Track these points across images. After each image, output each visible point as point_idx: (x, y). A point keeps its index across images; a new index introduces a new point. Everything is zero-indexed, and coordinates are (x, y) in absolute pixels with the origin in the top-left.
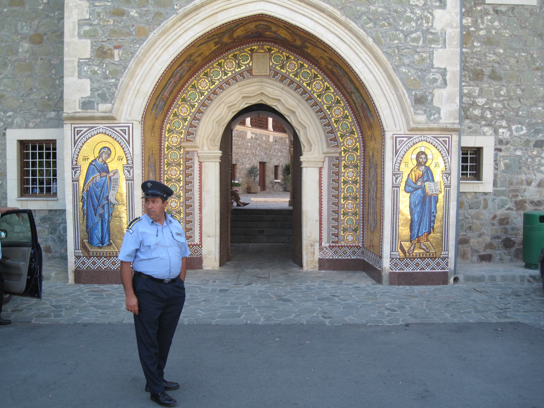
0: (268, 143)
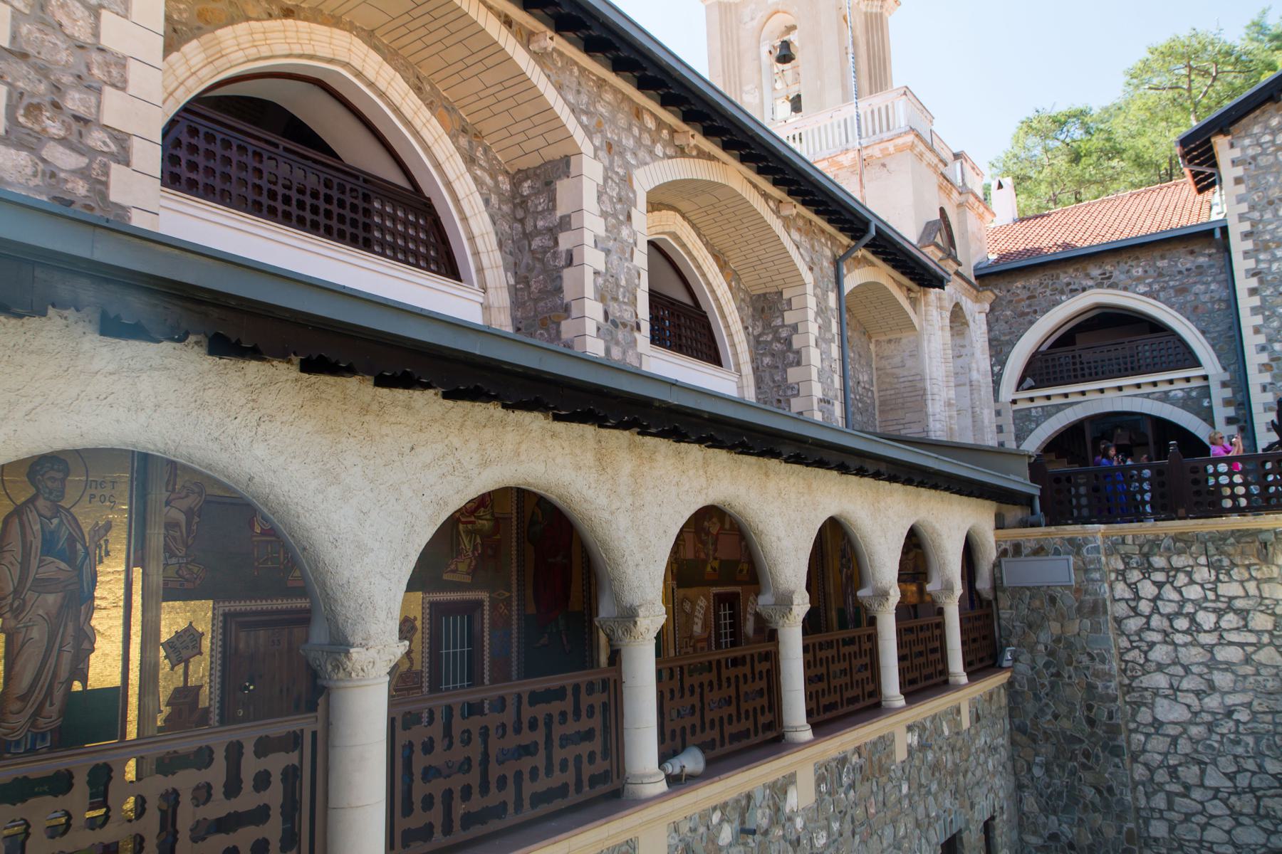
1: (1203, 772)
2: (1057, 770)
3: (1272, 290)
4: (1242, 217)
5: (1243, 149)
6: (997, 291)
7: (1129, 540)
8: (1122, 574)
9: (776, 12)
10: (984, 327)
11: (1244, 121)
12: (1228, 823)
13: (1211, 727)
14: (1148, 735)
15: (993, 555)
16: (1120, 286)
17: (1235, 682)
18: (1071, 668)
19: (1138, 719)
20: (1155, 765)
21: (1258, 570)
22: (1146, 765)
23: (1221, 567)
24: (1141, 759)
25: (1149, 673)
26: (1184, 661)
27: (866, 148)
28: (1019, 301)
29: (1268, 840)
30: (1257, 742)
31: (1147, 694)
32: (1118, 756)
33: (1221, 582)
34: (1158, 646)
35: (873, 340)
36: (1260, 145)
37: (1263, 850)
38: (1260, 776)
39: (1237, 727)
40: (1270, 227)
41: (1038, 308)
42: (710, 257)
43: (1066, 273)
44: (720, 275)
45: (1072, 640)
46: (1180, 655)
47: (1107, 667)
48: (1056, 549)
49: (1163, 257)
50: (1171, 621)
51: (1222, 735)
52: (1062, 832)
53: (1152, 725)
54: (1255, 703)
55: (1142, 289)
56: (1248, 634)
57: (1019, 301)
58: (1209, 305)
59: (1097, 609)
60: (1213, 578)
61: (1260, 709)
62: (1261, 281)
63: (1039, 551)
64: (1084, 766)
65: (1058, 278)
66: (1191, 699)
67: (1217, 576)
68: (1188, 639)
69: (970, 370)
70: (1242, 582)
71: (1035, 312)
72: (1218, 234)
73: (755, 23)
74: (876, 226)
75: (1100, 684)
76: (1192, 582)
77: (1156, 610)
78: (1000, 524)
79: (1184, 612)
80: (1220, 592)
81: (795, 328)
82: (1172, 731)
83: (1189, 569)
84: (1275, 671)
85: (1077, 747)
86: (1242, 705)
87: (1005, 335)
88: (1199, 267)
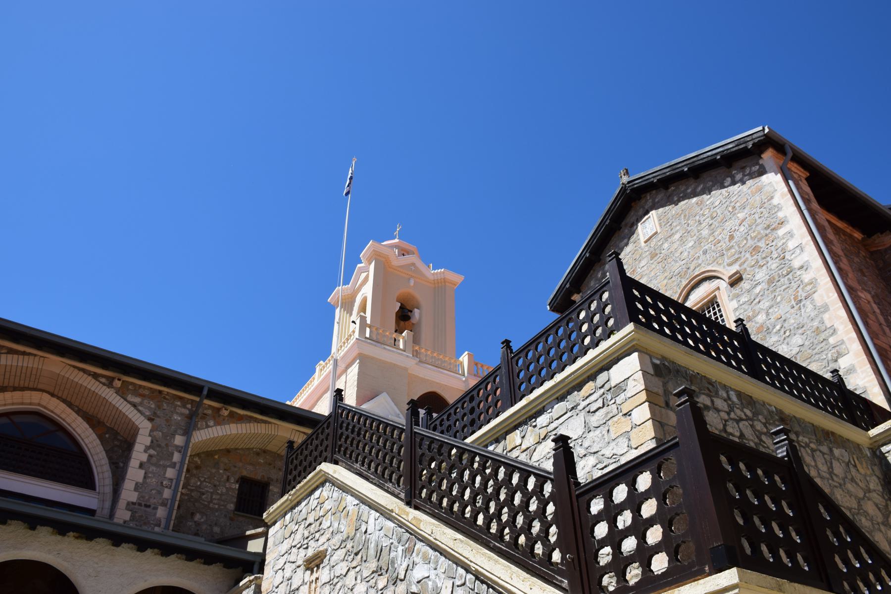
42: (80, 419)
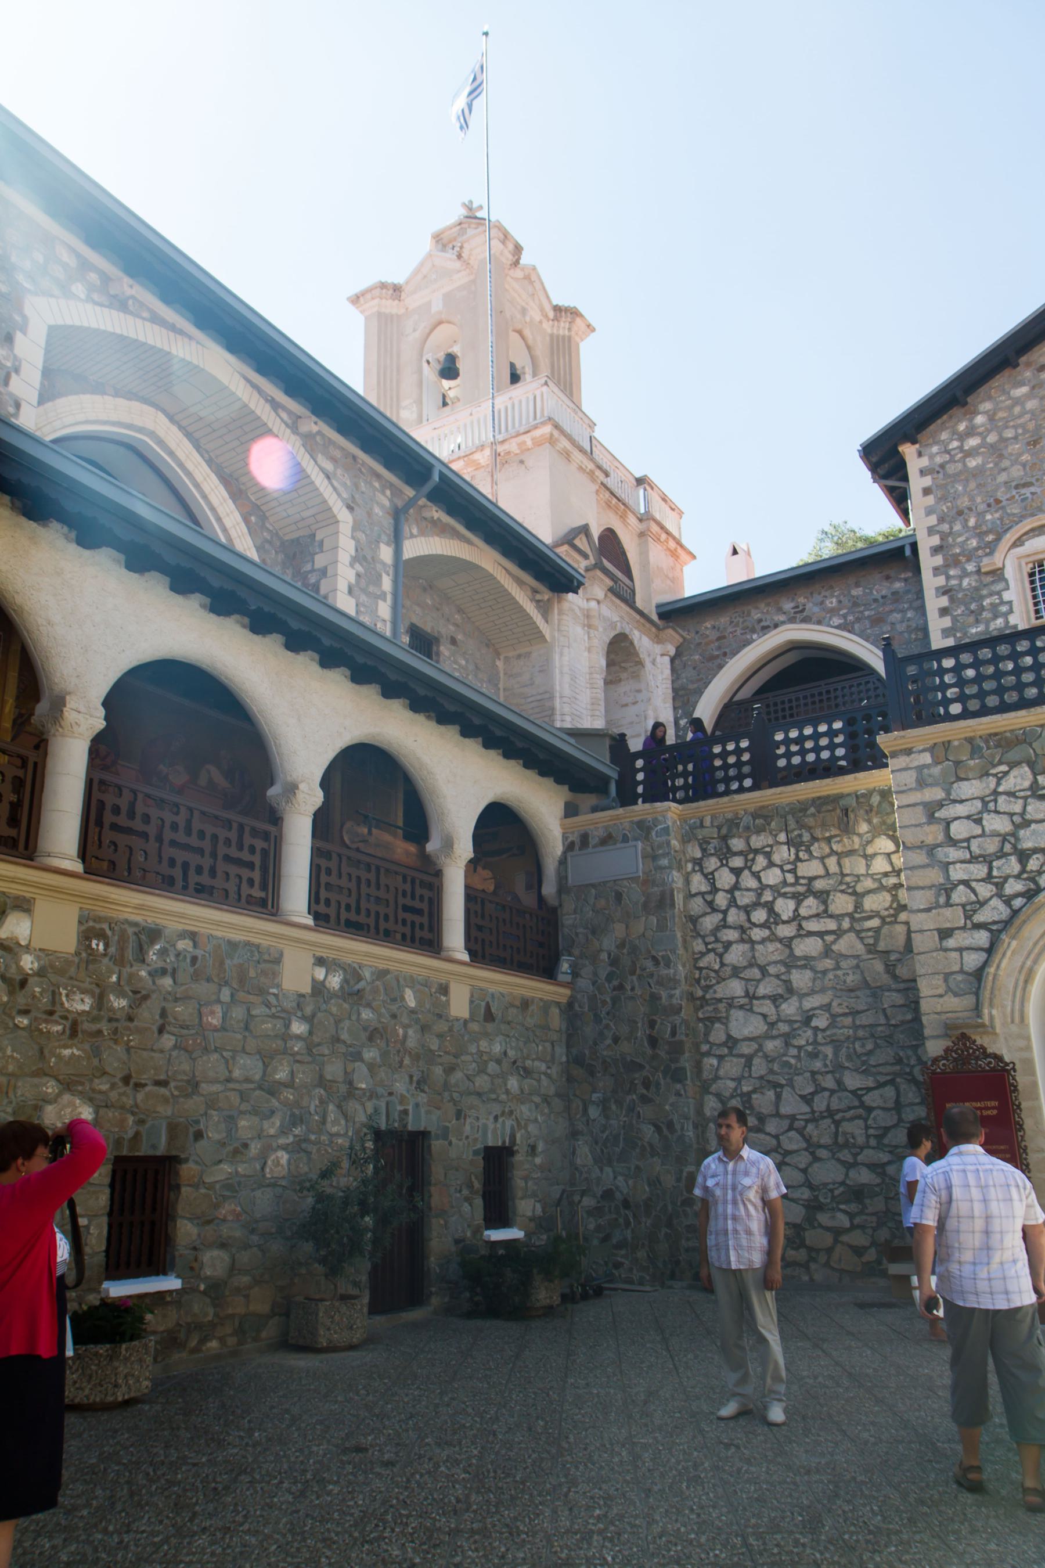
0: (442, 1027)
1: (778, 1096)
2: (614, 1107)
3: (963, 608)
4: (931, 531)
5: (932, 457)
6: (685, 634)
7: (707, 821)
8: (698, 863)
9: (440, 323)
10: (668, 672)
11: (932, 427)
12: (803, 1160)
13: (787, 1039)
14: (721, 1058)
15: (559, 849)
16: (814, 619)
17: (814, 980)
18: (635, 978)
19: (711, 1039)
20: (727, 1094)
21: (839, 842)
22: (718, 1095)
23: (802, 843)
24: (713, 1088)
25: (724, 980)
26: (761, 961)
27: (503, 442)
28: (707, 644)
29: (847, 1175)
30: (836, 1054)
31: (722, 1006)
32: (680, 1081)
33: (801, 861)
34: (734, 946)
35: (502, 657)
36: (948, 452)
37: (841, 1189)
38: (839, 1094)
39: (816, 1035)
40: (960, 540)
41: (727, 650)
42: (213, 477)
43: (757, 608)
44: (230, 502)
45: (637, 942)
46: (757, 955)
47: (672, 971)
48: (625, 835)
49: (857, 585)
50: (748, 914)
51: (800, 1048)
52: (617, 1188)
53: (724, 1044)
54: (834, 1004)
55: (836, 621)
56: (828, 920)
57: (707, 644)
58: (906, 635)
59: (664, 901)
60: (793, 857)
61: (840, 1011)
62: (952, 600)
63: (607, 840)
64: (645, 1100)
65: (749, 614)
66: (767, 1008)
67: (797, 855)
68: (766, 933)
69: (646, 718)
70: (822, 859)
71: (725, 654)
72: (908, 552)
73: (417, 335)
74: (441, 472)
75: (664, 995)
76: (771, 864)
77: (733, 902)
78: (571, 810)
79: (762, 901)
80: (799, 874)
81: (324, 572)
82: (746, 1049)
83: (768, 849)
84: (855, 962)
85: (637, 1075)
86: (820, 1008)
87: (692, 682)
88: (894, 593)
